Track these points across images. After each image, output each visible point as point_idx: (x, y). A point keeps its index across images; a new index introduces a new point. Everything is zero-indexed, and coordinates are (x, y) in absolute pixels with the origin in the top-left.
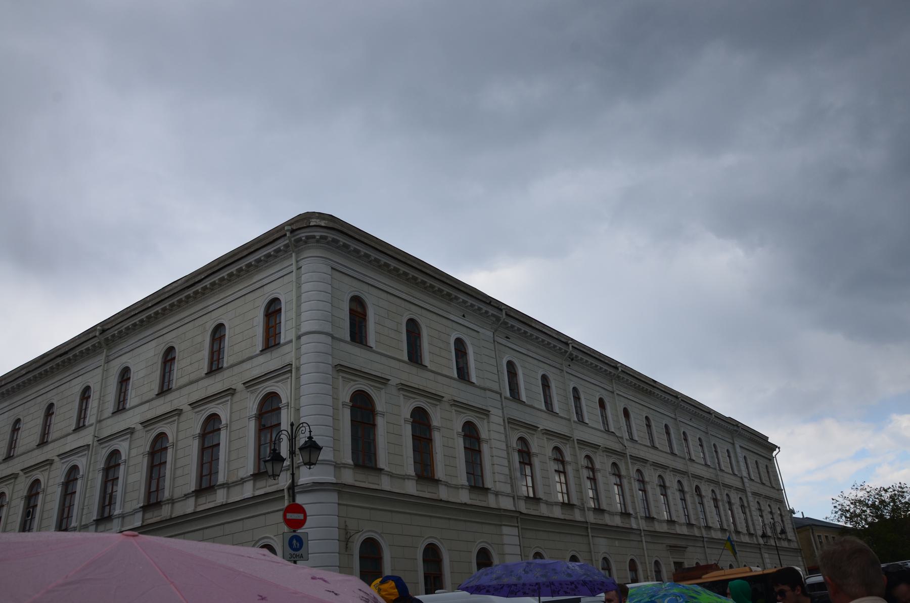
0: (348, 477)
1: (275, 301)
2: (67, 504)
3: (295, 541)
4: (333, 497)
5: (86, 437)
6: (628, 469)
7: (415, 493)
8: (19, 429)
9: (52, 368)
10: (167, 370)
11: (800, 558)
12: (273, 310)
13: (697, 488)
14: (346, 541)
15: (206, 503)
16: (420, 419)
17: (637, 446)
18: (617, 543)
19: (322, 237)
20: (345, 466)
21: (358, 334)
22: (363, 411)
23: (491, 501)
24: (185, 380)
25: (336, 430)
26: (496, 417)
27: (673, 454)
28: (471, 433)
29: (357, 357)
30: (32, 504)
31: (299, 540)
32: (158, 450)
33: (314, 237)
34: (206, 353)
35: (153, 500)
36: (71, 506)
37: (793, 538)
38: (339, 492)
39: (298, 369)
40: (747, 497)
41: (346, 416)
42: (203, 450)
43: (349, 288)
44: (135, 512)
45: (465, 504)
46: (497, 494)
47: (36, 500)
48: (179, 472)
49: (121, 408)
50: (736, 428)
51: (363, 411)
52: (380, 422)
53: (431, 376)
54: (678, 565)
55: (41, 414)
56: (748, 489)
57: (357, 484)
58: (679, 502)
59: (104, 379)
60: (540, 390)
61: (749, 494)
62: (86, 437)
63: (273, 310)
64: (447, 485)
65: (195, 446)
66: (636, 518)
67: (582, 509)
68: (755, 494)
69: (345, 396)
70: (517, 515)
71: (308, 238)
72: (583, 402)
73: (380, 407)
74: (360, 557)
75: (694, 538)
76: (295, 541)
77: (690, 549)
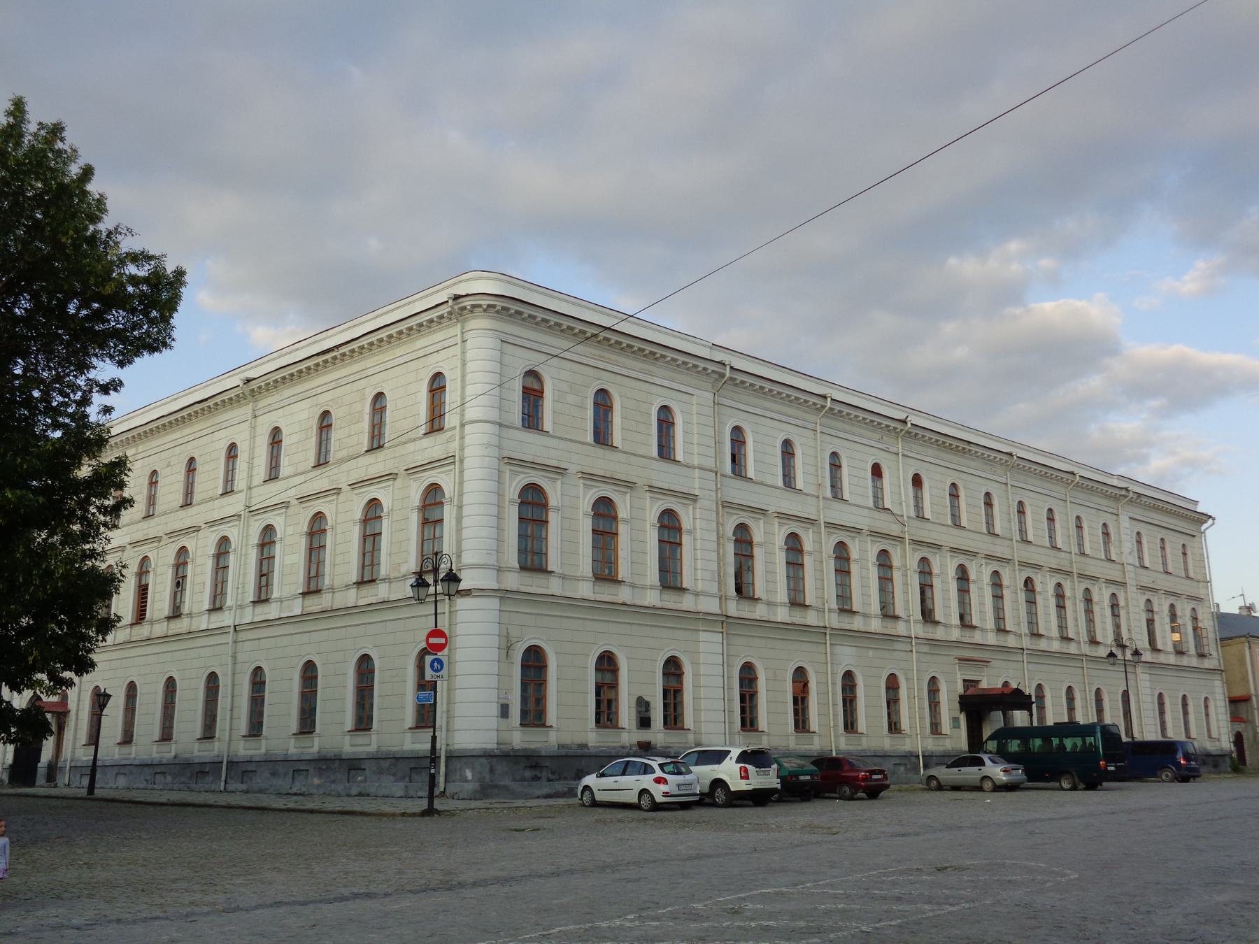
0: (513, 581)
1: (438, 375)
2: (220, 579)
4: (494, 603)
5: (234, 504)
6: (904, 556)
7: (591, 596)
8: (156, 482)
9: (190, 415)
10: (324, 437)
11: (1218, 683)
12: (437, 385)
13: (1028, 582)
14: (508, 649)
15: (369, 595)
16: (604, 510)
17: (928, 526)
18: (871, 653)
19: (489, 306)
20: (510, 570)
21: (532, 419)
22: (533, 505)
23: (687, 603)
24: (344, 453)
25: (500, 529)
26: (707, 501)
27: (991, 533)
28: (669, 524)
29: (529, 445)
30: (180, 574)
31: (440, 662)
32: (317, 529)
33: (480, 306)
34: (365, 424)
35: (313, 588)
36: (224, 582)
38: (501, 598)
39: (462, 461)
40: (1126, 592)
41: (512, 514)
42: (365, 537)
43: (521, 361)
44: (293, 598)
45: (654, 608)
46: (697, 594)
47: (185, 570)
48: (339, 559)
49: (273, 474)
50: (1123, 492)
51: (533, 505)
52: (553, 517)
53: (623, 457)
54: (968, 683)
55: (182, 468)
57: (523, 589)
58: (989, 600)
59: (253, 437)
60: (778, 460)
61: (1132, 589)
62: (234, 504)
63: (437, 385)
64: (633, 586)
65: (356, 532)
66: (908, 621)
67: (821, 611)
68: (1144, 588)
69: (512, 491)
70: (723, 619)
71: (474, 306)
72: (845, 471)
73: (553, 501)
74: (523, 666)
75: (1008, 650)
77: (994, 663)
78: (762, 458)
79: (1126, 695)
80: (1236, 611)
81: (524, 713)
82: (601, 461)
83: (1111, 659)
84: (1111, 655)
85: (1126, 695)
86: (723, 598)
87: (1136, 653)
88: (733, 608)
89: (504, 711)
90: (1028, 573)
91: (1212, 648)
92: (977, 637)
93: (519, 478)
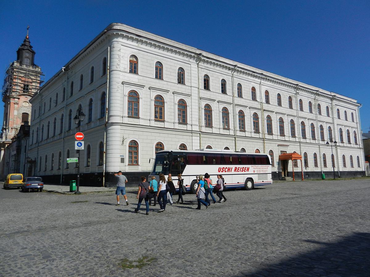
3: (79, 144)
11: (361, 152)
23: (189, 128)
26: (195, 97)
37: (360, 144)
56: (336, 123)
61: (336, 125)
76: (79, 144)
78: (215, 85)
79: (333, 156)
80: (368, 132)
81: (129, 161)
82: (158, 83)
83: (327, 144)
84: (327, 143)
85: (333, 156)
86: (200, 127)
87: (335, 142)
88: (204, 129)
89: (122, 161)
90: (302, 120)
91: (360, 142)
92: (287, 139)
93: (128, 88)
